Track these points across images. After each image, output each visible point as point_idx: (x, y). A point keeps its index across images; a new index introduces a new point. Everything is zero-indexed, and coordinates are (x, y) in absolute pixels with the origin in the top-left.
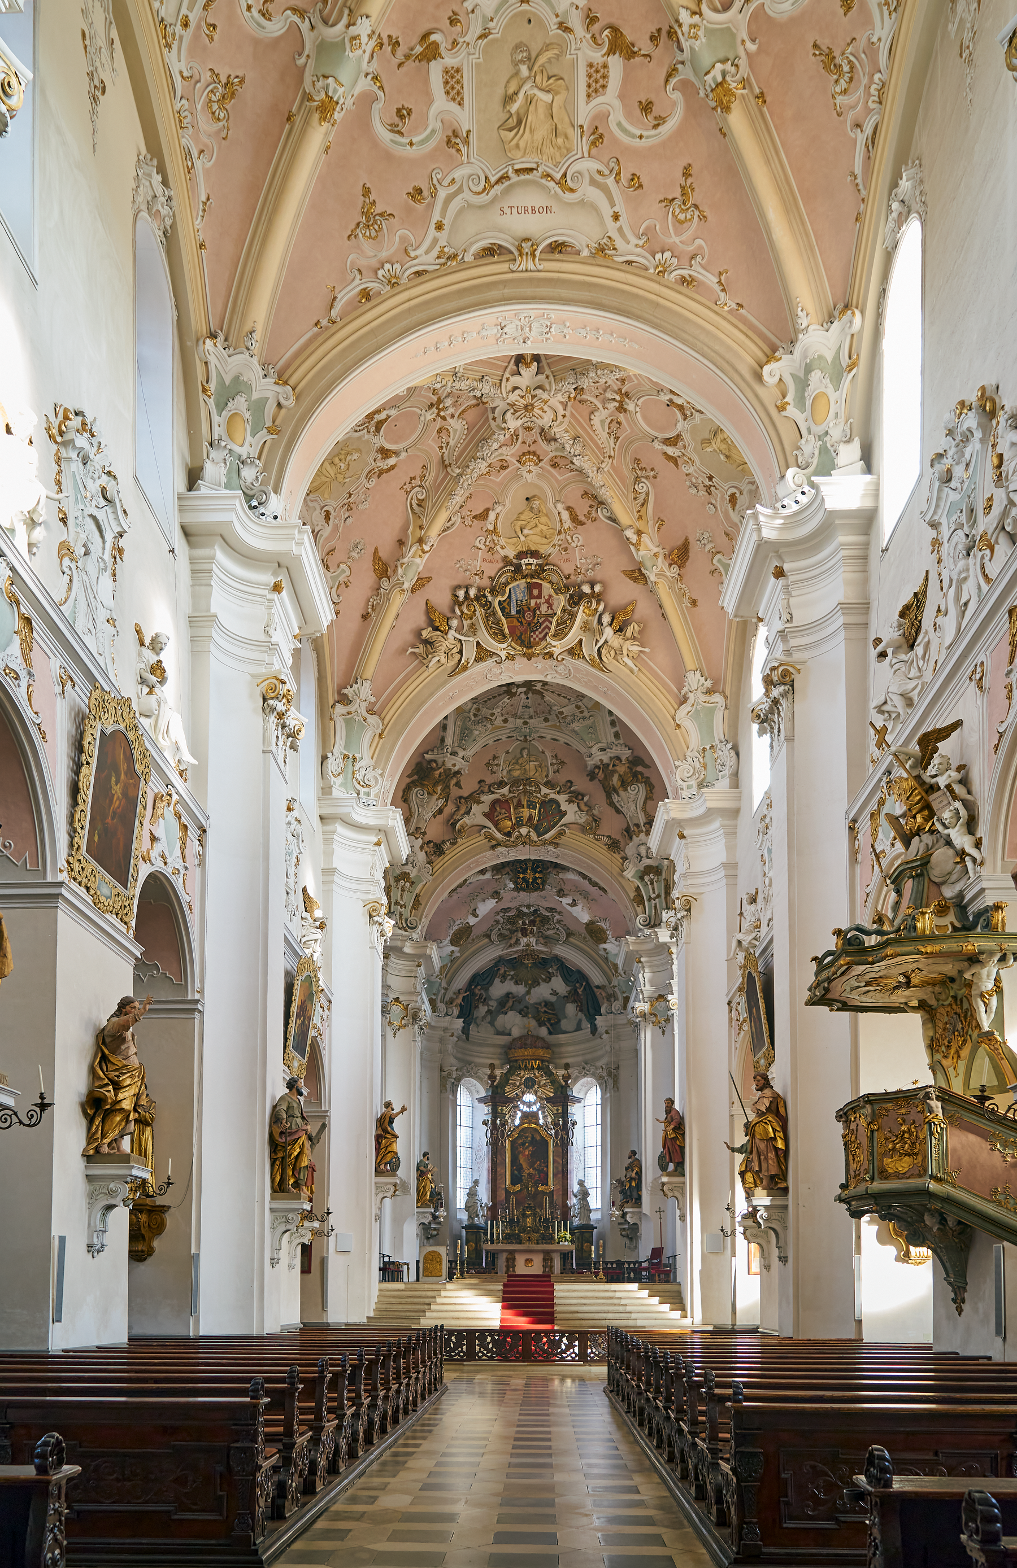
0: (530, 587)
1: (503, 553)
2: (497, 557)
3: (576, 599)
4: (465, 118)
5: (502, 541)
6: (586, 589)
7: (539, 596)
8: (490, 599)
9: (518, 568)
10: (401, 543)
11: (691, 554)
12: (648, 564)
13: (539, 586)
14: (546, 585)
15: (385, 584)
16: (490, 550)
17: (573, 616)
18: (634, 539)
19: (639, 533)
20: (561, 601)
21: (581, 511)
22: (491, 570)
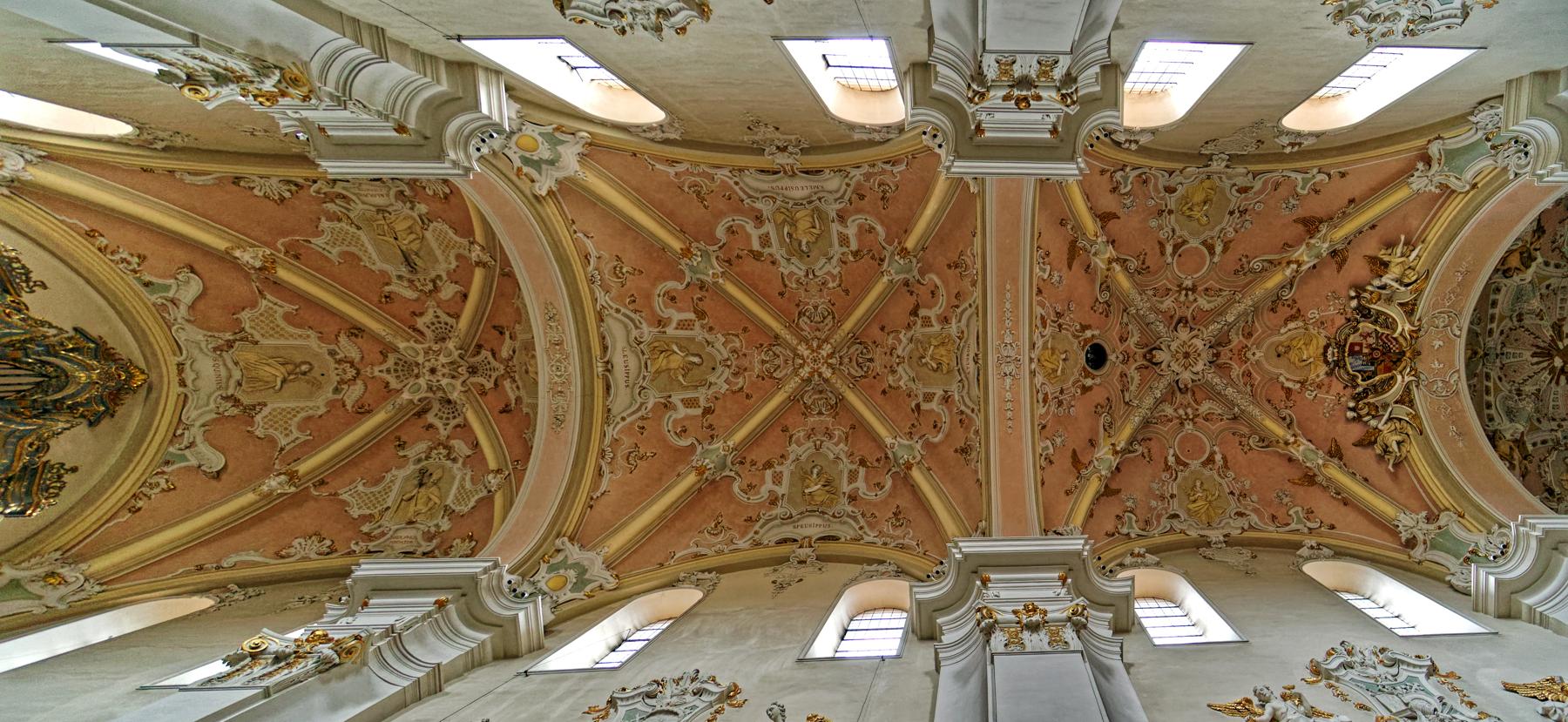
0: (1352, 353)
1: (1322, 376)
2: (1326, 381)
3: (1364, 312)
4: (940, 393)
5: (1313, 376)
6: (1354, 303)
7: (1361, 345)
8: (1360, 389)
9: (1337, 363)
10: (1290, 460)
11: (1307, 215)
12: (1315, 252)
13: (1352, 345)
14: (1351, 340)
15: (1319, 479)
16: (1319, 387)
17: (1379, 313)
18: (1294, 266)
19: (1289, 263)
20: (1365, 326)
21: (1285, 312)
22: (1337, 386)
